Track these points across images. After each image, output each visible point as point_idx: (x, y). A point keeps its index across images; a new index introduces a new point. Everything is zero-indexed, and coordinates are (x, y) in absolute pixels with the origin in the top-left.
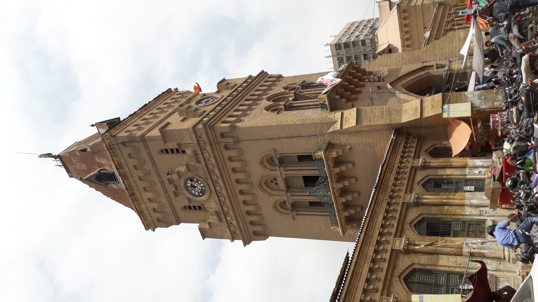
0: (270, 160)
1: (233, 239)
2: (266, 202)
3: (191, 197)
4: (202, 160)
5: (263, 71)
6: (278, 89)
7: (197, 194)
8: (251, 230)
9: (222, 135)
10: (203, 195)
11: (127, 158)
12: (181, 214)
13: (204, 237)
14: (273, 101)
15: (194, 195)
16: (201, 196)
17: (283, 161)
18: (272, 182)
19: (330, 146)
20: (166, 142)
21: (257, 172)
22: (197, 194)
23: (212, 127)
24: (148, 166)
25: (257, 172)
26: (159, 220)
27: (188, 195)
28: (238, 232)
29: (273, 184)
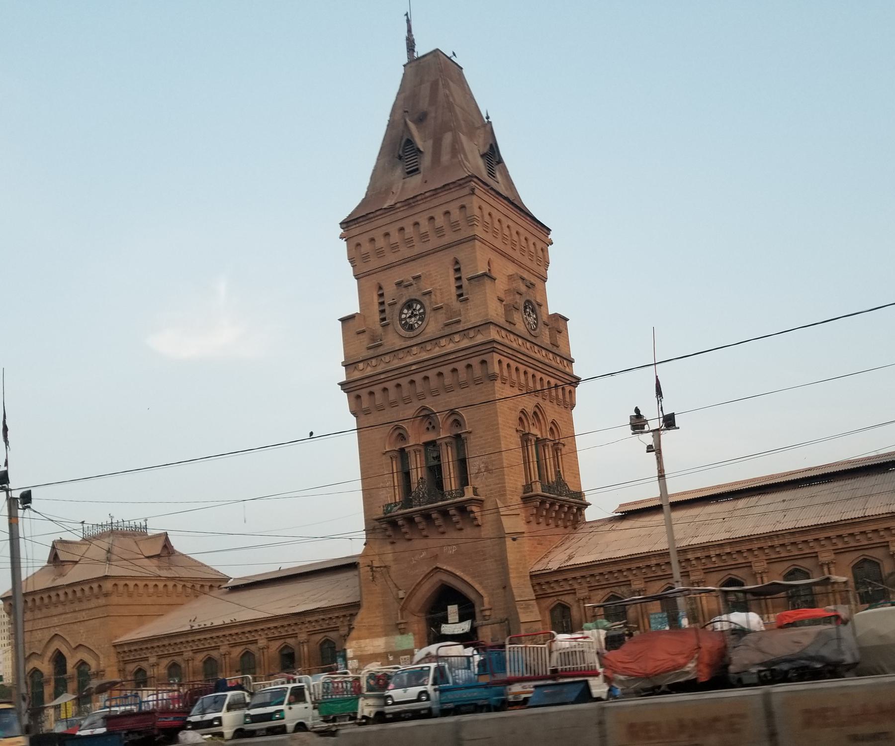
0: (457, 423)
1: (346, 365)
3: (399, 306)
4: (448, 331)
6: (551, 412)
7: (403, 316)
10: (403, 326)
13: (344, 320)
14: (535, 413)
15: (401, 313)
16: (400, 323)
17: (459, 440)
18: (430, 423)
20: (470, 279)
22: (403, 316)
24: (434, 242)
28: (357, 375)
29: (427, 425)
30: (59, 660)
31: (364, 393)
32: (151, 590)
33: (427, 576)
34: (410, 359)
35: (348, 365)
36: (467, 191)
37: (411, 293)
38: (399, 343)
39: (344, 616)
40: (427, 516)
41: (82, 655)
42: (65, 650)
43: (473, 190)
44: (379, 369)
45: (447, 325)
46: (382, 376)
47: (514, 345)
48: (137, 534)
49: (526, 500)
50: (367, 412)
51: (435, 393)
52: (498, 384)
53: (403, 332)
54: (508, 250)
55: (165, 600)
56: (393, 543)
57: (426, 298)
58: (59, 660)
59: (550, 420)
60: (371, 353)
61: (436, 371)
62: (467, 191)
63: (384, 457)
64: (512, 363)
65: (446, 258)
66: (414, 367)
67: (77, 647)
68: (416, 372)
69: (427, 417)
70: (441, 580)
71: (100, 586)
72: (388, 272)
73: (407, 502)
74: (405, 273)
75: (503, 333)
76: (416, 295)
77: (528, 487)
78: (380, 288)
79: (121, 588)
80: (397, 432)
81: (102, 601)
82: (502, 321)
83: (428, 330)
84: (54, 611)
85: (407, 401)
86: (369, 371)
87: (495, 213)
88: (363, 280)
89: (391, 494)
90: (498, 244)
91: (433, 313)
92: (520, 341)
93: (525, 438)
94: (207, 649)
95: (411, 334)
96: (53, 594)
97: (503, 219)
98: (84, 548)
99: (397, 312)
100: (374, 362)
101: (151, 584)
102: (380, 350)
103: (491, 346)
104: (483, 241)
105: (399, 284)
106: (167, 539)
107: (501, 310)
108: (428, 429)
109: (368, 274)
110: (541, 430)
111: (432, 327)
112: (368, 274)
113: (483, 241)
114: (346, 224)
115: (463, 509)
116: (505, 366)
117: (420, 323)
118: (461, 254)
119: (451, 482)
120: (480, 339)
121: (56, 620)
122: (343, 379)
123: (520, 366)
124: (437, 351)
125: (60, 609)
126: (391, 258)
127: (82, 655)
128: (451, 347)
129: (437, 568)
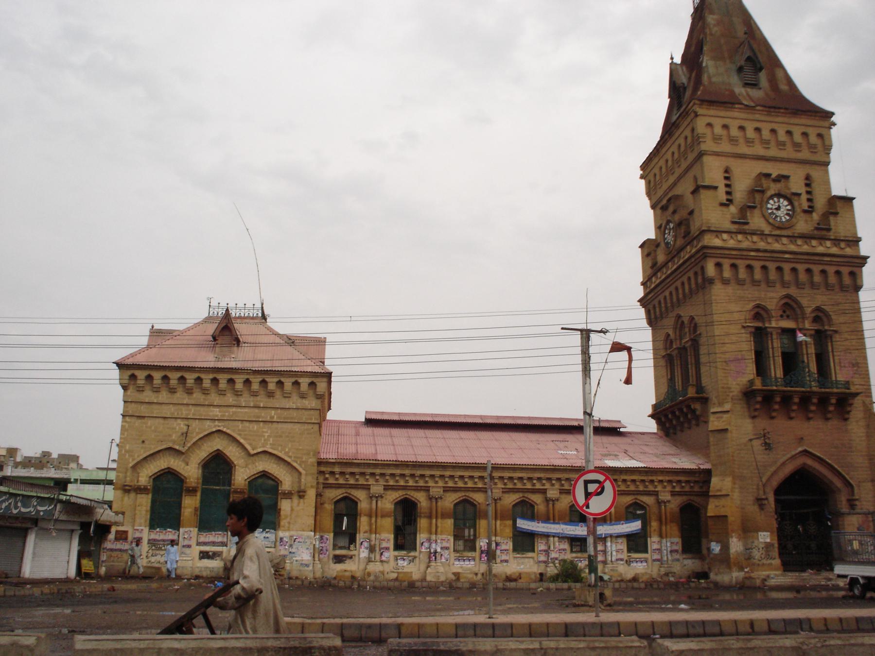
2: (772, 298)
17: (821, 337)
21: (809, 301)
22: (769, 206)
25: (809, 301)
27: (769, 193)
29: (780, 313)
33: (793, 457)
34: (777, 246)
39: (670, 481)
40: (786, 399)
46: (753, 254)
56: (754, 417)
57: (796, 198)
61: (807, 266)
63: (743, 331)
66: (787, 256)
68: (787, 261)
69: (790, 307)
70: (804, 464)
72: (740, 161)
74: (775, 170)
80: (757, 310)
85: (769, 284)
86: (731, 243)
91: (802, 214)
94: (467, 489)
108: (782, 316)
117: (788, 218)
129: (805, 451)
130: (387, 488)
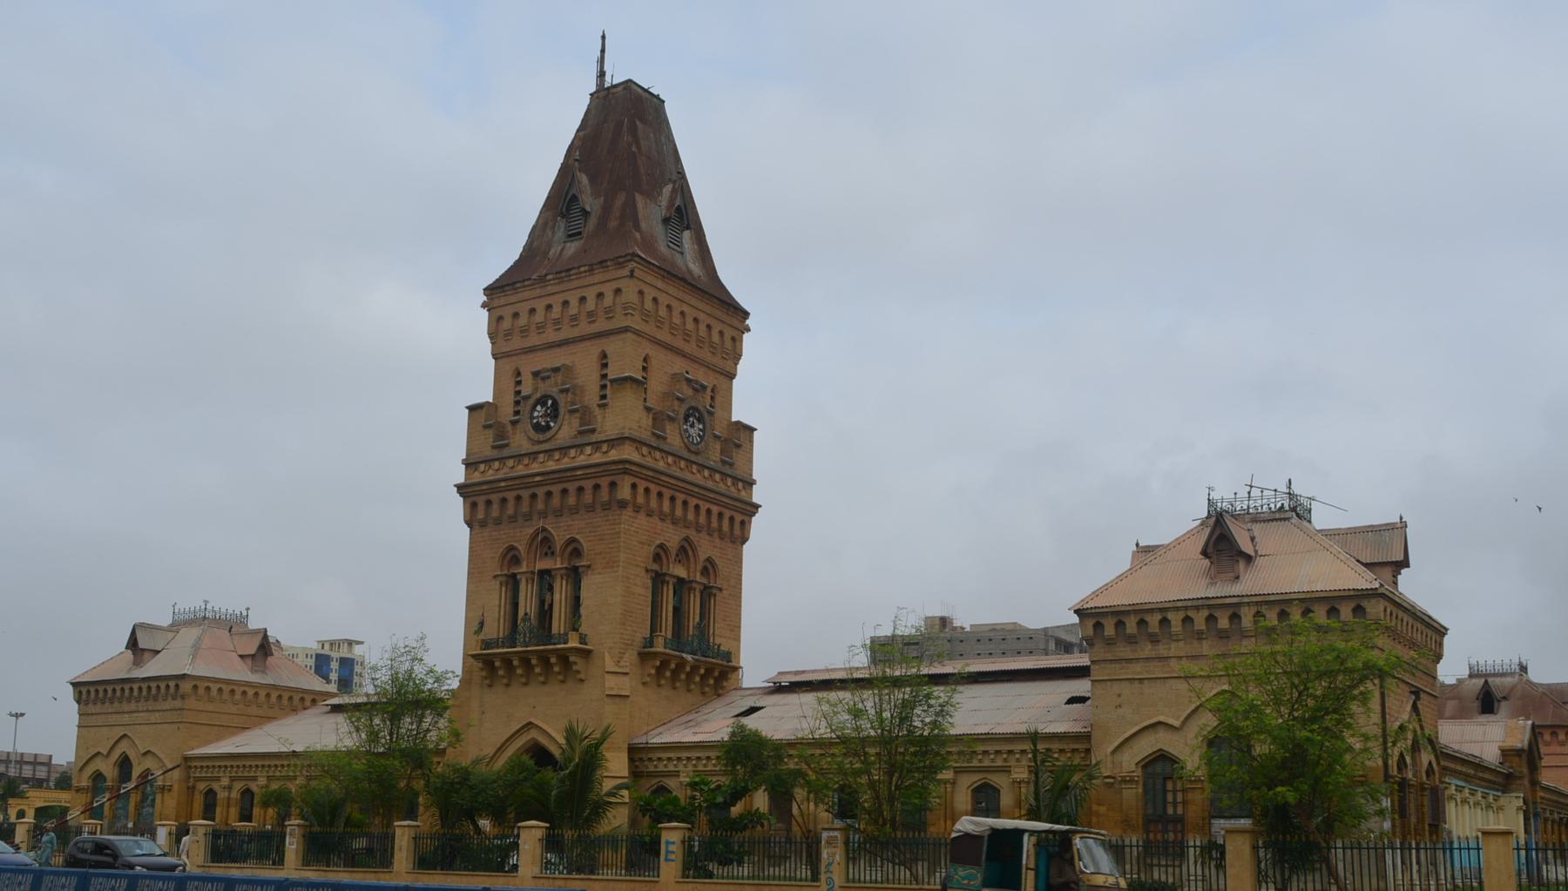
0: (577, 553)
2: (520, 536)
3: (532, 401)
4: (579, 441)
5: (757, 507)
6: (706, 548)
8: (481, 498)
9: (613, 485)
11: (597, 289)
12: (509, 366)
15: (534, 409)
17: (575, 576)
19: (586, 654)
23: (626, 472)
24: (584, 328)
26: (500, 318)
30: (125, 764)
31: (481, 500)
32: (238, 697)
34: (536, 468)
35: (470, 464)
36: (626, 272)
37: (550, 387)
38: (526, 447)
41: (149, 763)
42: (132, 755)
43: (632, 272)
44: (500, 475)
45: (580, 433)
47: (661, 465)
48: (233, 625)
49: (644, 657)
50: (483, 524)
51: (559, 513)
52: (629, 511)
53: (532, 433)
54: (678, 343)
55: (254, 710)
58: (125, 764)
59: (702, 556)
60: (495, 454)
62: (626, 272)
64: (652, 486)
65: (593, 349)
67: (145, 754)
68: (539, 484)
69: (544, 543)
71: (177, 686)
73: (511, 640)
75: (645, 450)
76: (554, 391)
77: (650, 642)
78: (519, 374)
79: (201, 691)
81: (178, 703)
82: (645, 435)
83: (561, 435)
84: (126, 707)
85: (528, 517)
87: (664, 300)
88: (501, 362)
89: (495, 628)
90: (663, 336)
92: (670, 459)
93: (658, 579)
95: (541, 437)
96: (127, 687)
97: (675, 304)
98: (170, 635)
99: (528, 408)
100: (496, 465)
101: (239, 690)
102: (506, 452)
103: (624, 467)
104: (637, 333)
105: (536, 374)
106: (265, 636)
107: (647, 421)
109: (507, 355)
110: (688, 569)
111: (566, 431)
112: (507, 355)
113: (637, 333)
114: (490, 291)
115: (564, 658)
116: (641, 490)
118: (612, 346)
119: (558, 624)
120: (614, 455)
121: (126, 718)
122: (461, 479)
123: (664, 490)
124: (566, 463)
125: (133, 706)
126: (534, 340)
127: (149, 763)
128: (582, 460)
130: (233, 779)
